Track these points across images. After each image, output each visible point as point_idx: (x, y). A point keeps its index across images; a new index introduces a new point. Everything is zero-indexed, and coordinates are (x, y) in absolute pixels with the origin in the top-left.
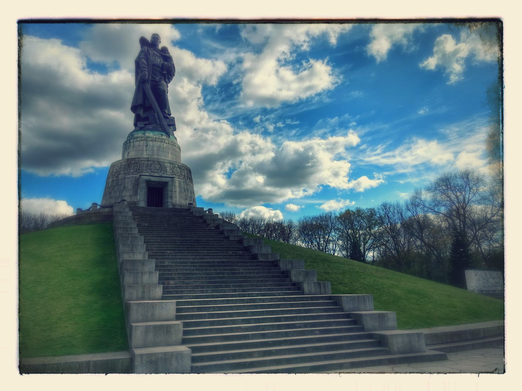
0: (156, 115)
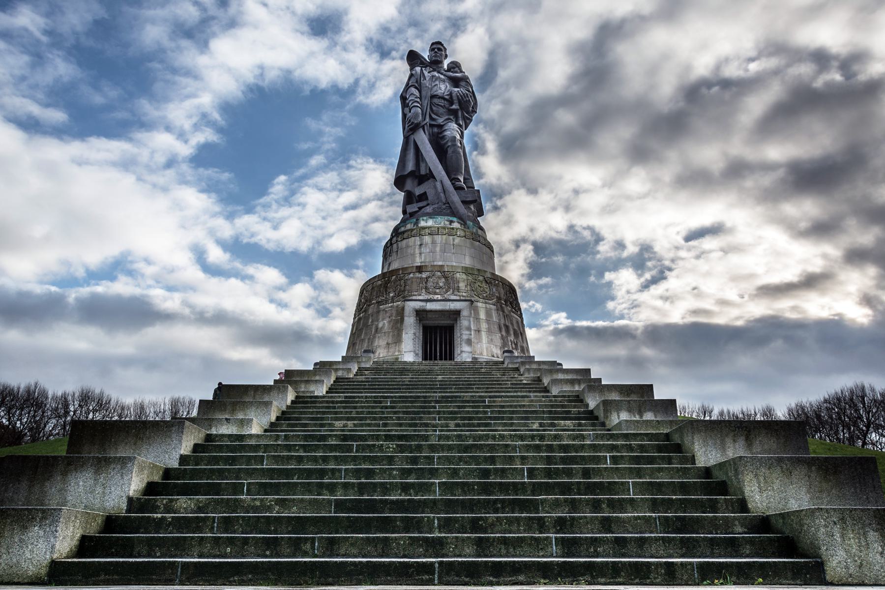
0: (438, 184)
